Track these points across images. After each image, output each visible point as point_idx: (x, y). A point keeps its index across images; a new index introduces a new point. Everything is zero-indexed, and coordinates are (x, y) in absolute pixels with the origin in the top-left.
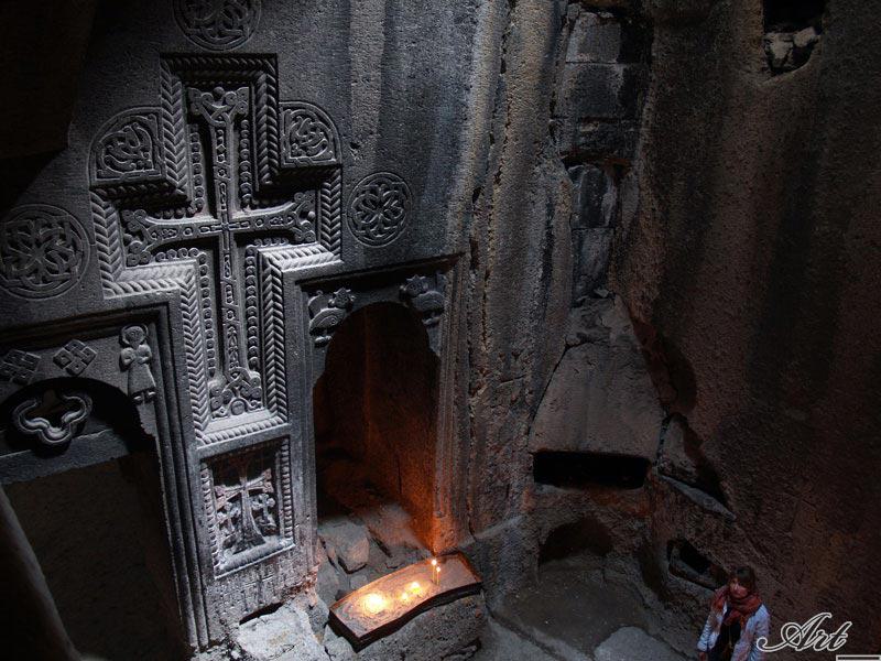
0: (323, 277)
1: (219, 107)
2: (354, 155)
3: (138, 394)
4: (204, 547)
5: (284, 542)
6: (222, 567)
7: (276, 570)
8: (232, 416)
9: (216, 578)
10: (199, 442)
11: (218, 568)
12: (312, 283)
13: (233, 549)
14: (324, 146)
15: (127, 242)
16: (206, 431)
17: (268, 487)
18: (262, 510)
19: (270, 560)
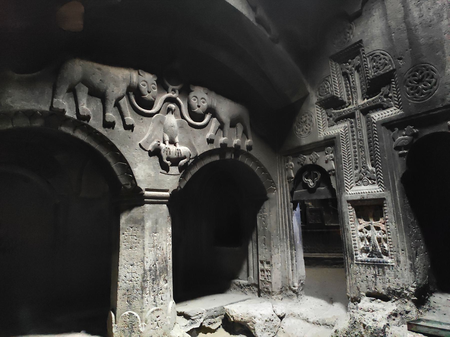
0: (394, 121)
1: (350, 67)
2: (400, 63)
3: (329, 171)
4: (350, 243)
5: (389, 261)
6: (359, 259)
7: (384, 273)
8: (363, 186)
9: (355, 262)
10: (347, 193)
11: (356, 258)
12: (389, 125)
13: (368, 254)
14: (386, 64)
15: (328, 120)
16: (351, 190)
17: (383, 227)
18: (380, 238)
19: (381, 266)
